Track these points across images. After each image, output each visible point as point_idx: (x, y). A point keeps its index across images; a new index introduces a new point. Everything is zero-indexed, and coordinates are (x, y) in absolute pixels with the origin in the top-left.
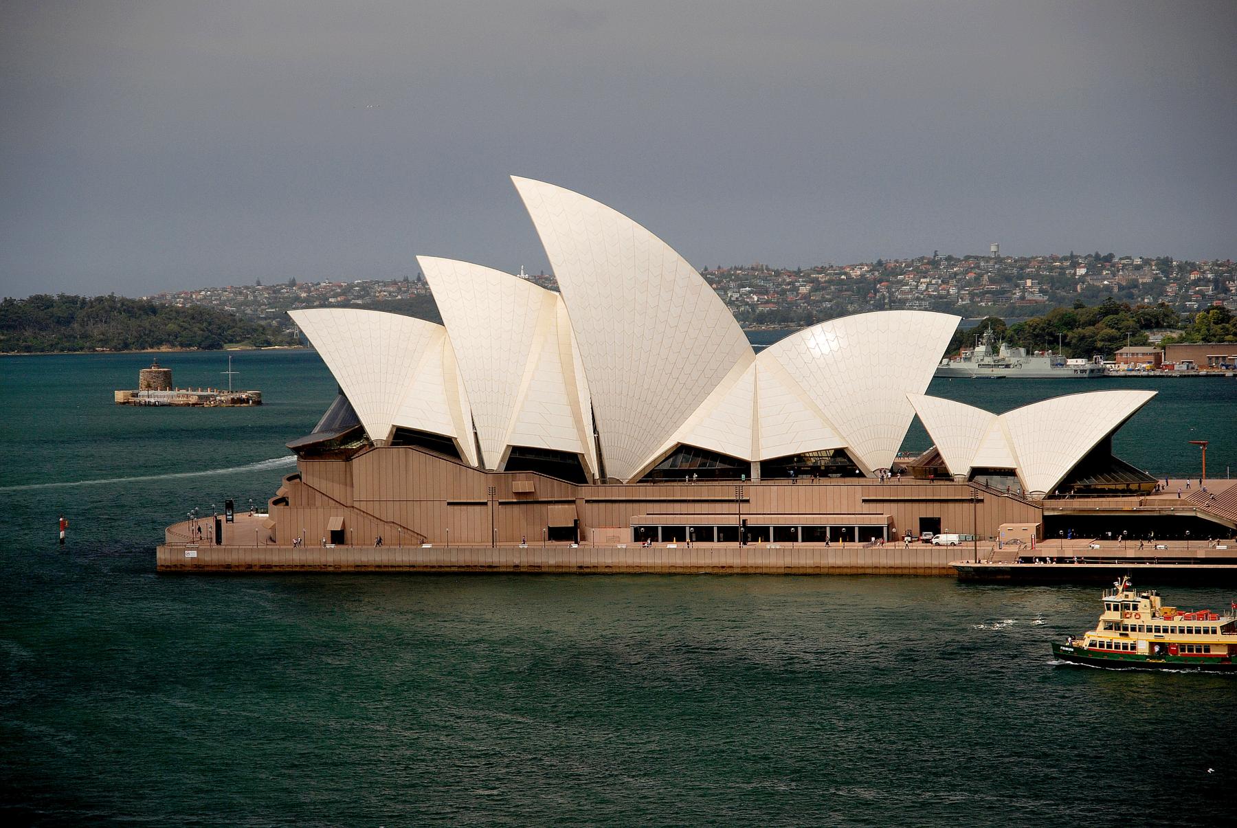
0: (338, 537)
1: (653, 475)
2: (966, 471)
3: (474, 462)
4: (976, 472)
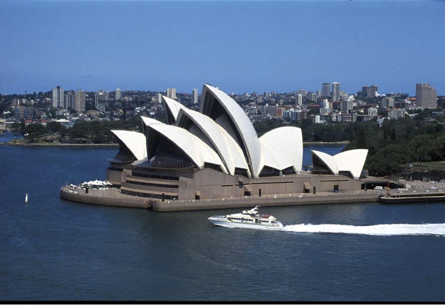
0: (197, 198)
1: (261, 175)
2: (338, 172)
3: (228, 173)
4: (341, 173)
